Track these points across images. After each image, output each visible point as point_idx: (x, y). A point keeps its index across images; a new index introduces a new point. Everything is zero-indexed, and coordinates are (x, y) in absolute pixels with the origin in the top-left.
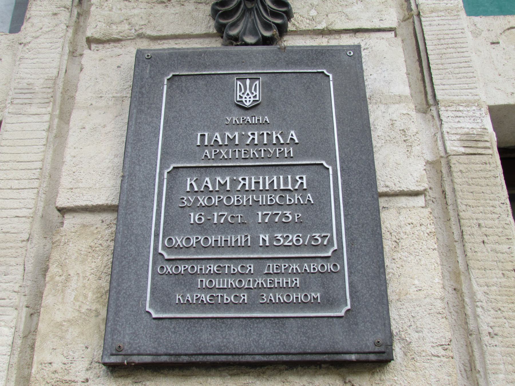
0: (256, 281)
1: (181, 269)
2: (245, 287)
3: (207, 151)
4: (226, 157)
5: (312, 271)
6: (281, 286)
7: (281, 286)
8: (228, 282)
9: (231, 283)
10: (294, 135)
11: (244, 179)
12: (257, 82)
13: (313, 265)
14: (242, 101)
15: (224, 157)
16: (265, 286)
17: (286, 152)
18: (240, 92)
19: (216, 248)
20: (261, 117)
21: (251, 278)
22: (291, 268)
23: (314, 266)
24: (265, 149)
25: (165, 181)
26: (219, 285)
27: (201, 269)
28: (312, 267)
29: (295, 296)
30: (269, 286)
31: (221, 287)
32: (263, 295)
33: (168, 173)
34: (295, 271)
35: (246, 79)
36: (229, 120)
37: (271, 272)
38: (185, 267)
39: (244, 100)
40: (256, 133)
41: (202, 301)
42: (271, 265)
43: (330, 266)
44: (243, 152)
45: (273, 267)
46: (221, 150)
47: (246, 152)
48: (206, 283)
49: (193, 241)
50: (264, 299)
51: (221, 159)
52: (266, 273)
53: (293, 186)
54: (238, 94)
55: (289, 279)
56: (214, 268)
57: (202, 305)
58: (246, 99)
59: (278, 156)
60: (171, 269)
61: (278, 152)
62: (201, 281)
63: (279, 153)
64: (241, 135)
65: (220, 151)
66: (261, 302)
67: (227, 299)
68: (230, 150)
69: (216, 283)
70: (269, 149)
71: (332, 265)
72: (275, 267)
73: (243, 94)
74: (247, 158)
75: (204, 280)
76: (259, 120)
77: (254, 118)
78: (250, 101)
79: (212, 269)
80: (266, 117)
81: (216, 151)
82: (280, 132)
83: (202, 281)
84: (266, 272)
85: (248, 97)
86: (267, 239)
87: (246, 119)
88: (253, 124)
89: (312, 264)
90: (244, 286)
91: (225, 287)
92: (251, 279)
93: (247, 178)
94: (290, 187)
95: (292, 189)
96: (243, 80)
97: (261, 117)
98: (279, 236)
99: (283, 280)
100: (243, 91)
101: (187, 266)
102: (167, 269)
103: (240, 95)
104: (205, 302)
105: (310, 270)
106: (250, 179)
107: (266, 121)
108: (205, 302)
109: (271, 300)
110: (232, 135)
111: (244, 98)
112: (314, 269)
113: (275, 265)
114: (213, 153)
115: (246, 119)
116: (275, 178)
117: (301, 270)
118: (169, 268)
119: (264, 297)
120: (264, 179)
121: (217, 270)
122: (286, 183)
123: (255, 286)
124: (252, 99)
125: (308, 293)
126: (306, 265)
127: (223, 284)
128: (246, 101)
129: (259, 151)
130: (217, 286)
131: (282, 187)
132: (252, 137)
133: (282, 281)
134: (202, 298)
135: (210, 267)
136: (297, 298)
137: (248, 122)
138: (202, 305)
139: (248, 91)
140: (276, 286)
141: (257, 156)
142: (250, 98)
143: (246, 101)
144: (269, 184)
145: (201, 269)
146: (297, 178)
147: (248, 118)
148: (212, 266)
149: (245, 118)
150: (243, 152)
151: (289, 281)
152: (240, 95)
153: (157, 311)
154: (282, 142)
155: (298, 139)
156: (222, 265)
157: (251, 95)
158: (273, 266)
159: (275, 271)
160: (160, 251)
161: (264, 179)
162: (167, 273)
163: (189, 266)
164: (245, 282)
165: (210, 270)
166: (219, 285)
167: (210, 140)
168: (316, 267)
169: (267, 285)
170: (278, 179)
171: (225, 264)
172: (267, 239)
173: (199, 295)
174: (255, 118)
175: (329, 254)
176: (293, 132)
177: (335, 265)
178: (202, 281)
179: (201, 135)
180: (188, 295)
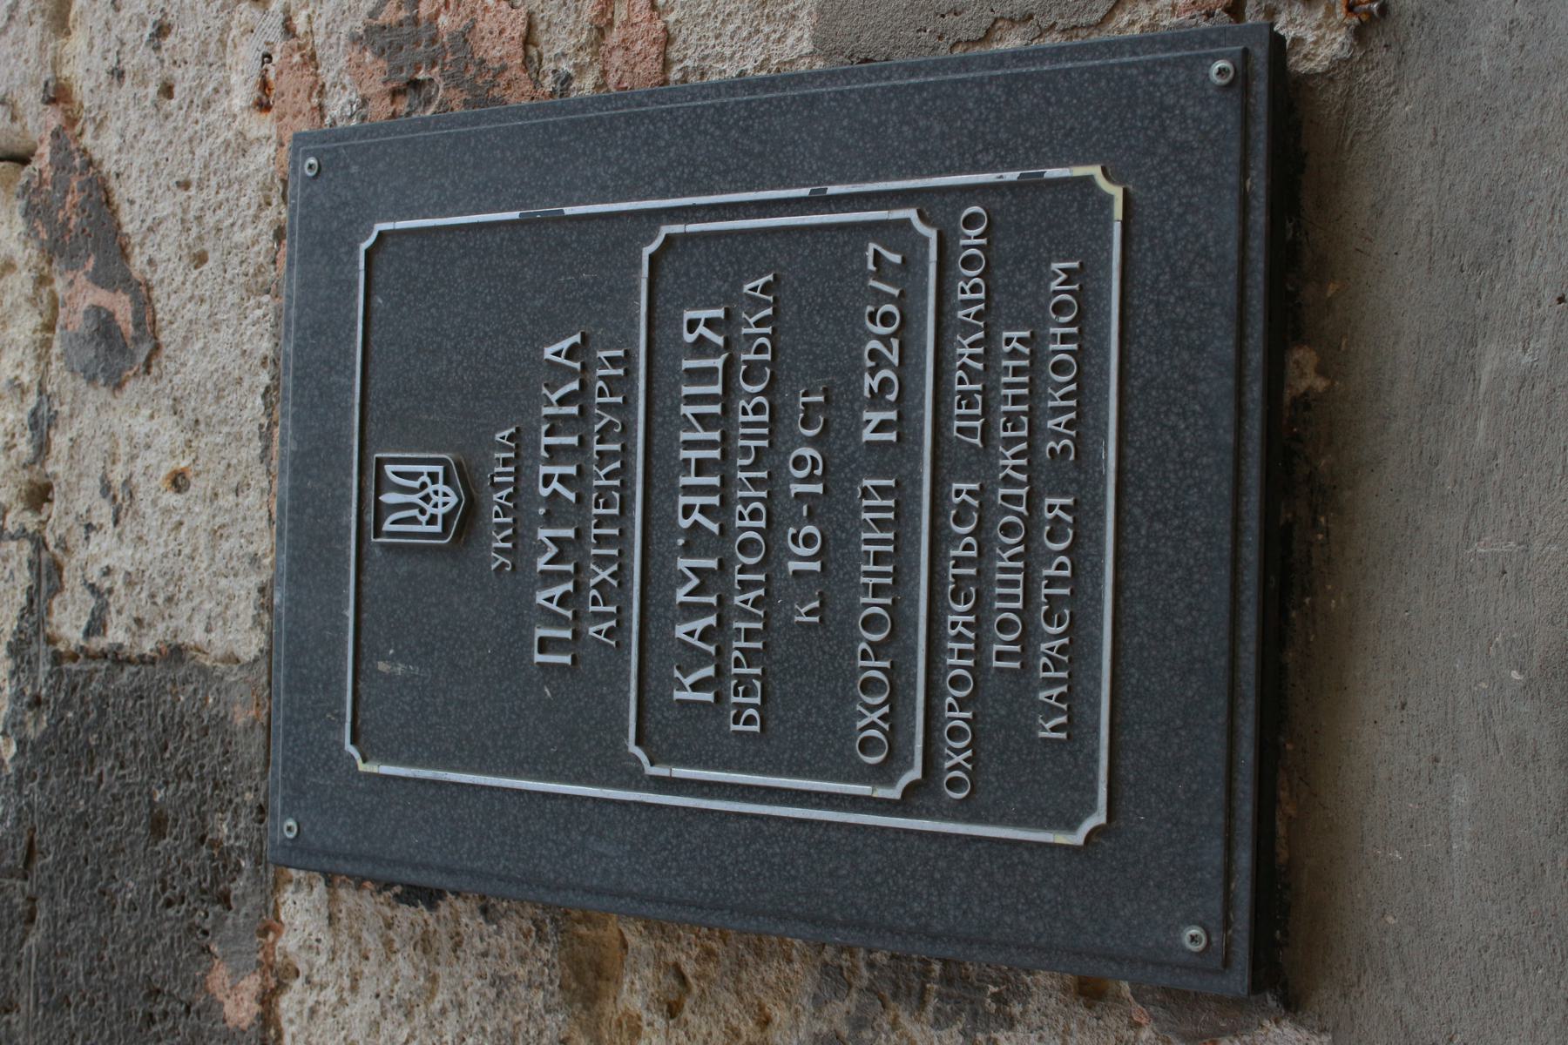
0: (1007, 475)
2: (1026, 513)
3: (592, 630)
4: (615, 568)
5: (981, 295)
6: (1025, 391)
7: (1025, 391)
8: (1004, 570)
9: (1011, 559)
10: (556, 347)
11: (688, 510)
12: (389, 469)
13: (963, 291)
14: (444, 516)
15: (611, 575)
16: (1024, 446)
17: (611, 372)
18: (419, 523)
20: (496, 455)
21: (995, 492)
22: (970, 362)
23: (967, 288)
24: (597, 437)
25: (681, 772)
26: (1014, 598)
27: (962, 654)
28: (969, 296)
29: (1059, 346)
30: (1024, 433)
31: (1019, 591)
32: (1052, 450)
33: (652, 764)
34: (980, 350)
35: (377, 502)
36: (502, 559)
37: (978, 424)
38: (951, 708)
39: (440, 511)
40: (544, 470)
41: (1062, 650)
42: (957, 423)
43: (969, 238)
44: (601, 511)
45: (965, 419)
46: (593, 582)
47: (601, 501)
48: (1004, 642)
50: (1065, 449)
51: (620, 584)
52: (983, 440)
53: (717, 351)
55: (1005, 363)
56: (959, 613)
57: (1077, 651)
58: (440, 505)
59: (619, 400)
60: (958, 752)
61: (607, 399)
62: (998, 659)
63: (611, 396)
64: (549, 520)
65: (596, 587)
66: (1072, 457)
67: (1061, 566)
68: (594, 552)
69: (1007, 608)
70: (597, 427)
71: (968, 232)
72: (963, 411)
73: (423, 512)
74: (621, 497)
75: (997, 647)
76: (506, 462)
77: (496, 479)
78: (445, 495)
79: (961, 619)
80: (498, 436)
81: (594, 598)
82: (545, 391)
83: (1001, 656)
84: (977, 441)
85: (435, 498)
87: (501, 505)
88: (516, 479)
89: (961, 297)
90: (1019, 514)
91: (1020, 577)
92: (1002, 491)
93: (683, 500)
94: (718, 363)
95: (724, 356)
96: (381, 511)
97: (496, 455)
99: (1009, 386)
100: (415, 512)
101: (949, 700)
102: (957, 767)
103: (429, 523)
104: (1066, 640)
105: (978, 302)
106: (690, 490)
107: (510, 438)
108: (1066, 640)
109: (1069, 425)
110: (545, 549)
111: (435, 511)
112: (975, 289)
113: (957, 411)
114: (601, 608)
115: (501, 505)
116: (688, 410)
117: (977, 329)
119: (1058, 448)
120: (690, 445)
121: (965, 603)
122: (705, 375)
123: (1024, 477)
124: (441, 487)
125: (1050, 299)
126: (960, 314)
127: (1014, 584)
128: (445, 504)
129: (601, 458)
130: (1019, 605)
131: (717, 389)
132: (555, 485)
133: (1010, 384)
134: (1051, 649)
135: (954, 625)
136: (1065, 339)
137: (508, 498)
139: (415, 498)
140: (1025, 408)
141: (617, 465)
142: (436, 493)
143: (445, 504)
144: (705, 430)
145: (962, 654)
146: (690, 338)
147: (495, 497)
148: (951, 618)
149: (496, 508)
150: (601, 511)
151: (1011, 363)
152: (429, 523)
154: (575, 386)
155: (570, 336)
156: (951, 587)
157: (430, 489)
158: (962, 417)
159: (978, 411)
161: (690, 445)
162: (969, 766)
163: (946, 694)
164: (1008, 512)
165: (965, 625)
166: (1014, 598)
167: (559, 621)
169: (1019, 440)
170: (692, 400)
171: (947, 577)
173: (1044, 660)
174: (500, 474)
175: (932, 234)
176: (548, 353)
177: (971, 221)
178: (1001, 656)
179: (541, 651)
180: (1042, 695)
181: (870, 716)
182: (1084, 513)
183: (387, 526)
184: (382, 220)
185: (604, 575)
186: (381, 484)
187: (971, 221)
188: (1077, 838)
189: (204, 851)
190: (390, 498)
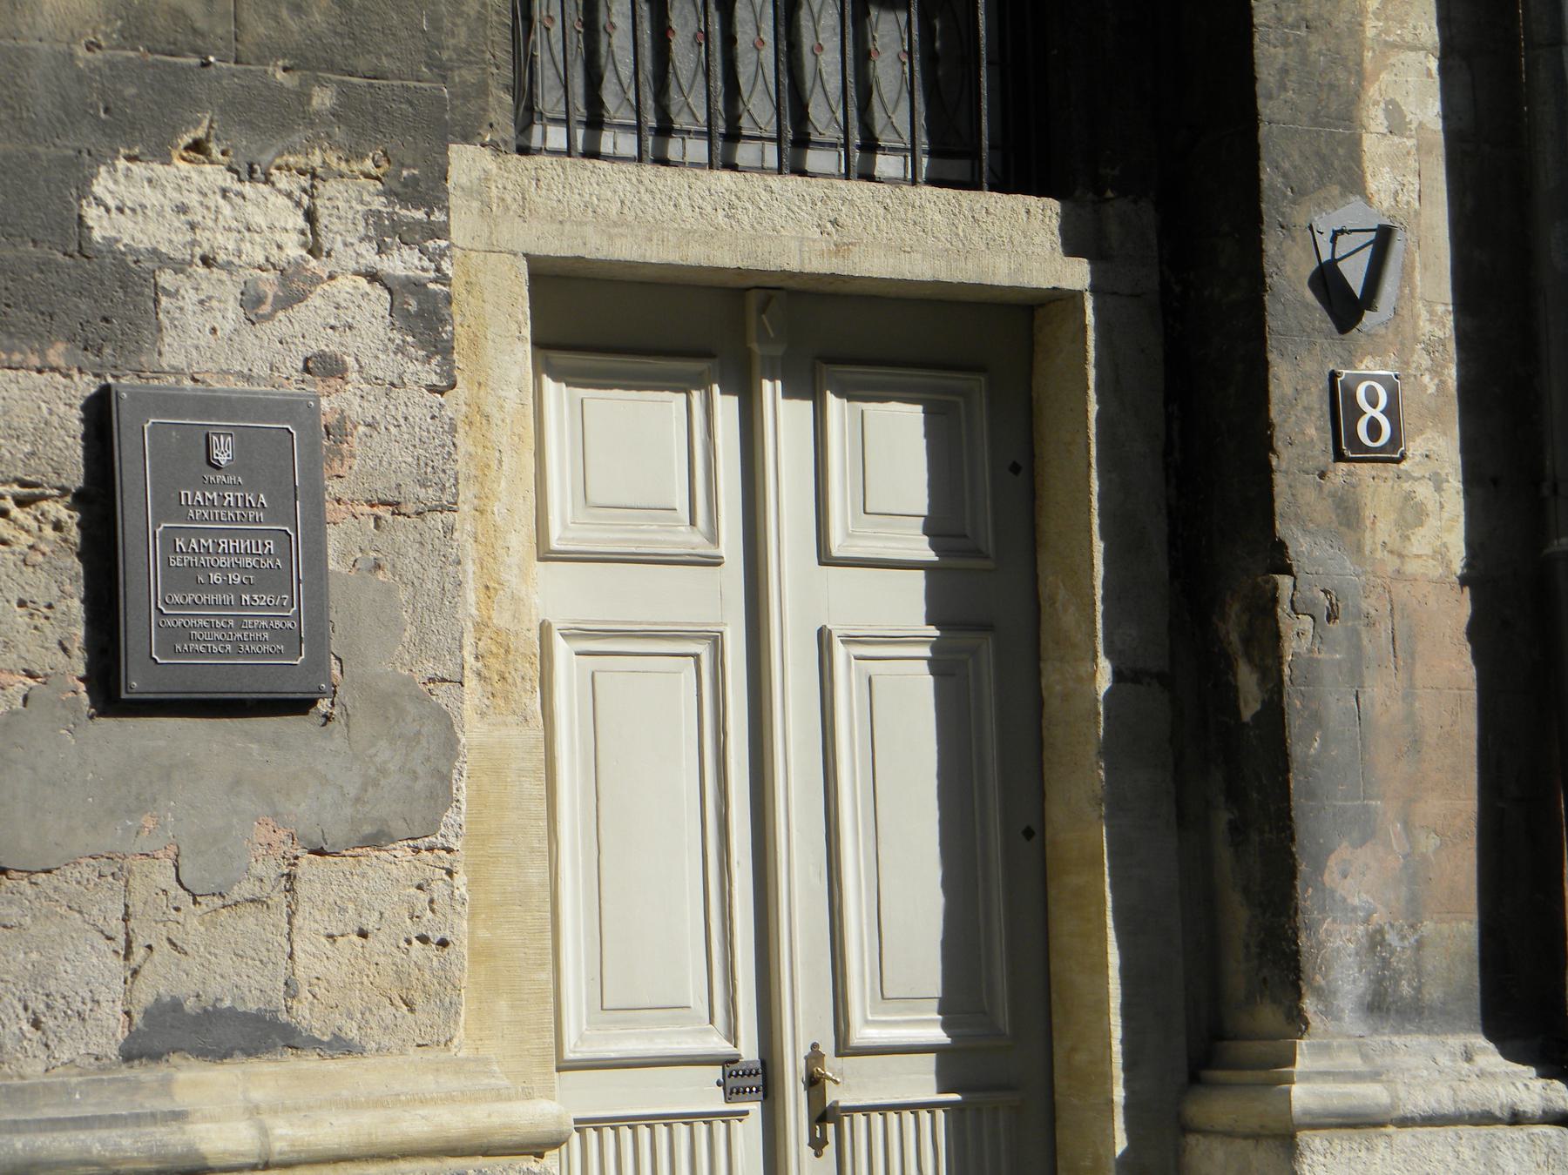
1: (179, 623)
19: (208, 605)
39: (219, 458)
40: (231, 494)
49: (189, 600)
54: (215, 452)
57: (197, 654)
86: (248, 599)
96: (218, 435)
98: (256, 597)
118: (170, 622)
138: (197, 654)
153: (161, 659)
160: (160, 606)
168: (278, 623)
172: (248, 599)
177: (293, 624)
181: (178, 598)
182: (227, 655)
183: (214, 438)
184: (297, 434)
185: (206, 515)
186: (226, 435)
187: (293, 624)
188: (154, 656)
189: (100, 341)
190: (222, 437)
